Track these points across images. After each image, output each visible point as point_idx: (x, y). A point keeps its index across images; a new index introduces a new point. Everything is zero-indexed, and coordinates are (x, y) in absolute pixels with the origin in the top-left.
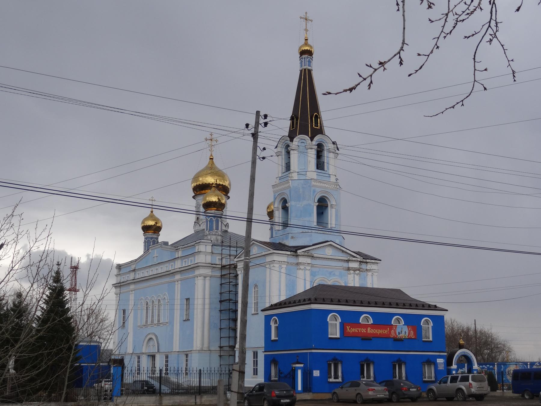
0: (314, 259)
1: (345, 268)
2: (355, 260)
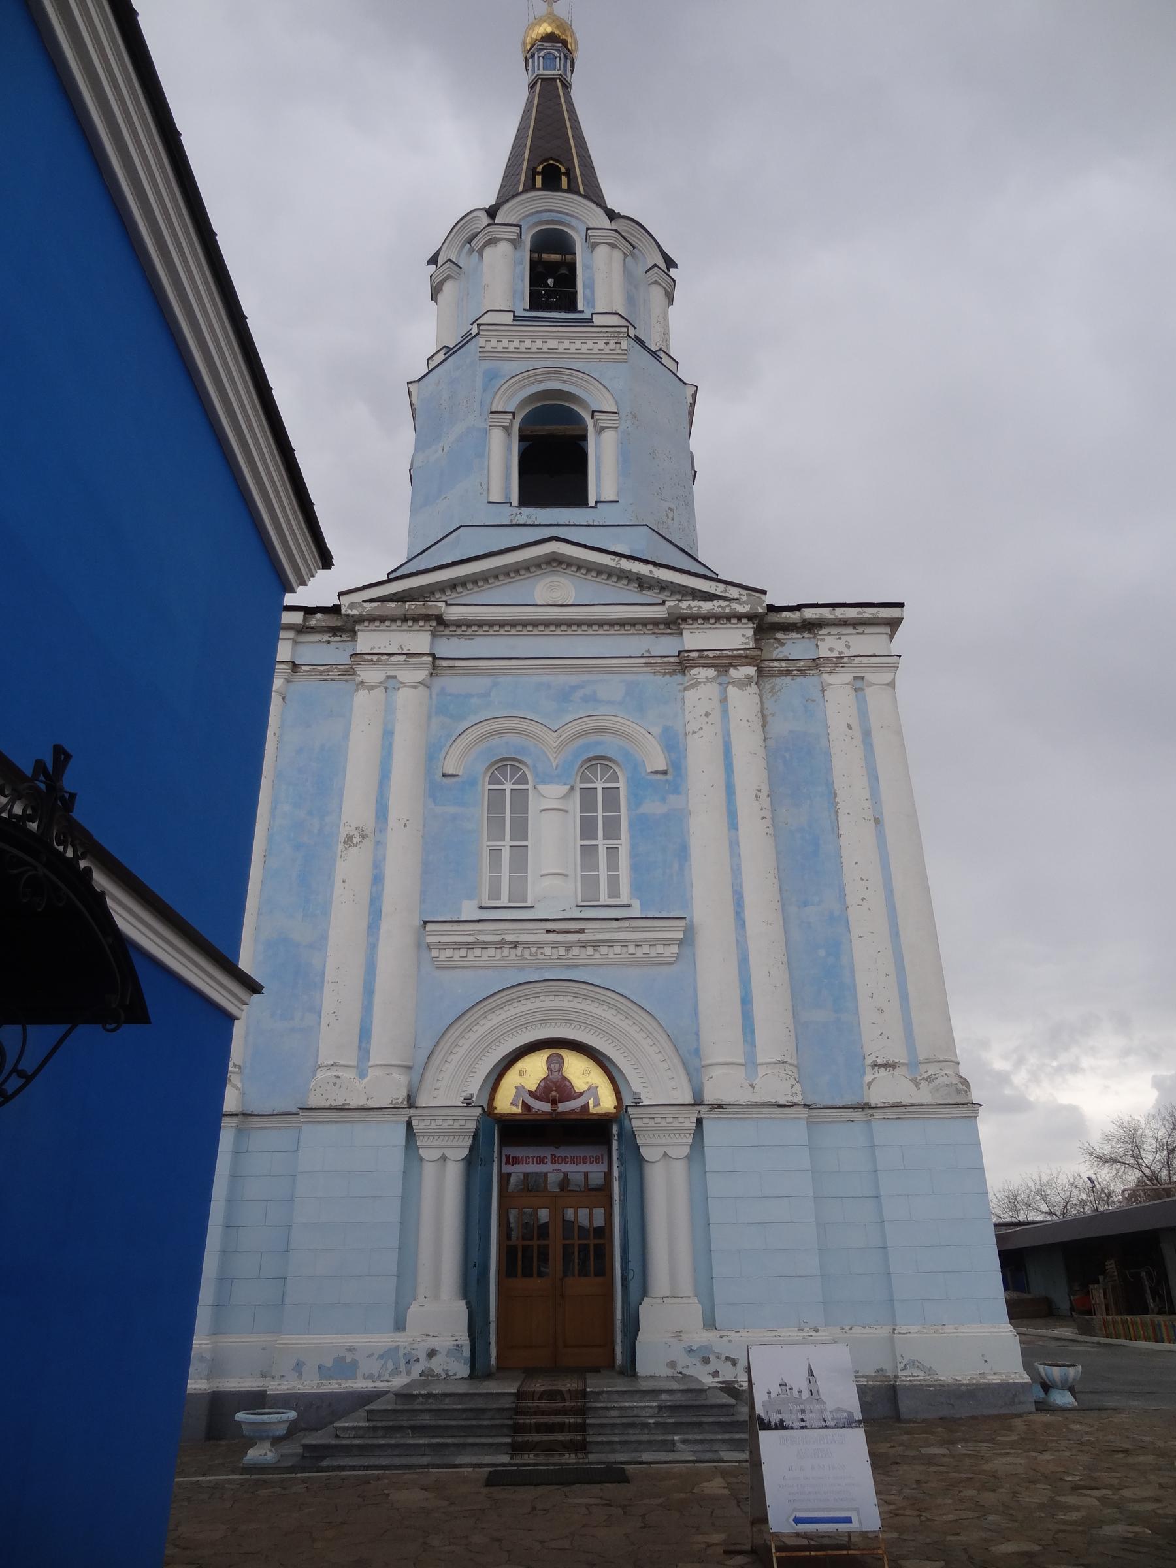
0: (460, 636)
1: (659, 660)
2: (717, 610)
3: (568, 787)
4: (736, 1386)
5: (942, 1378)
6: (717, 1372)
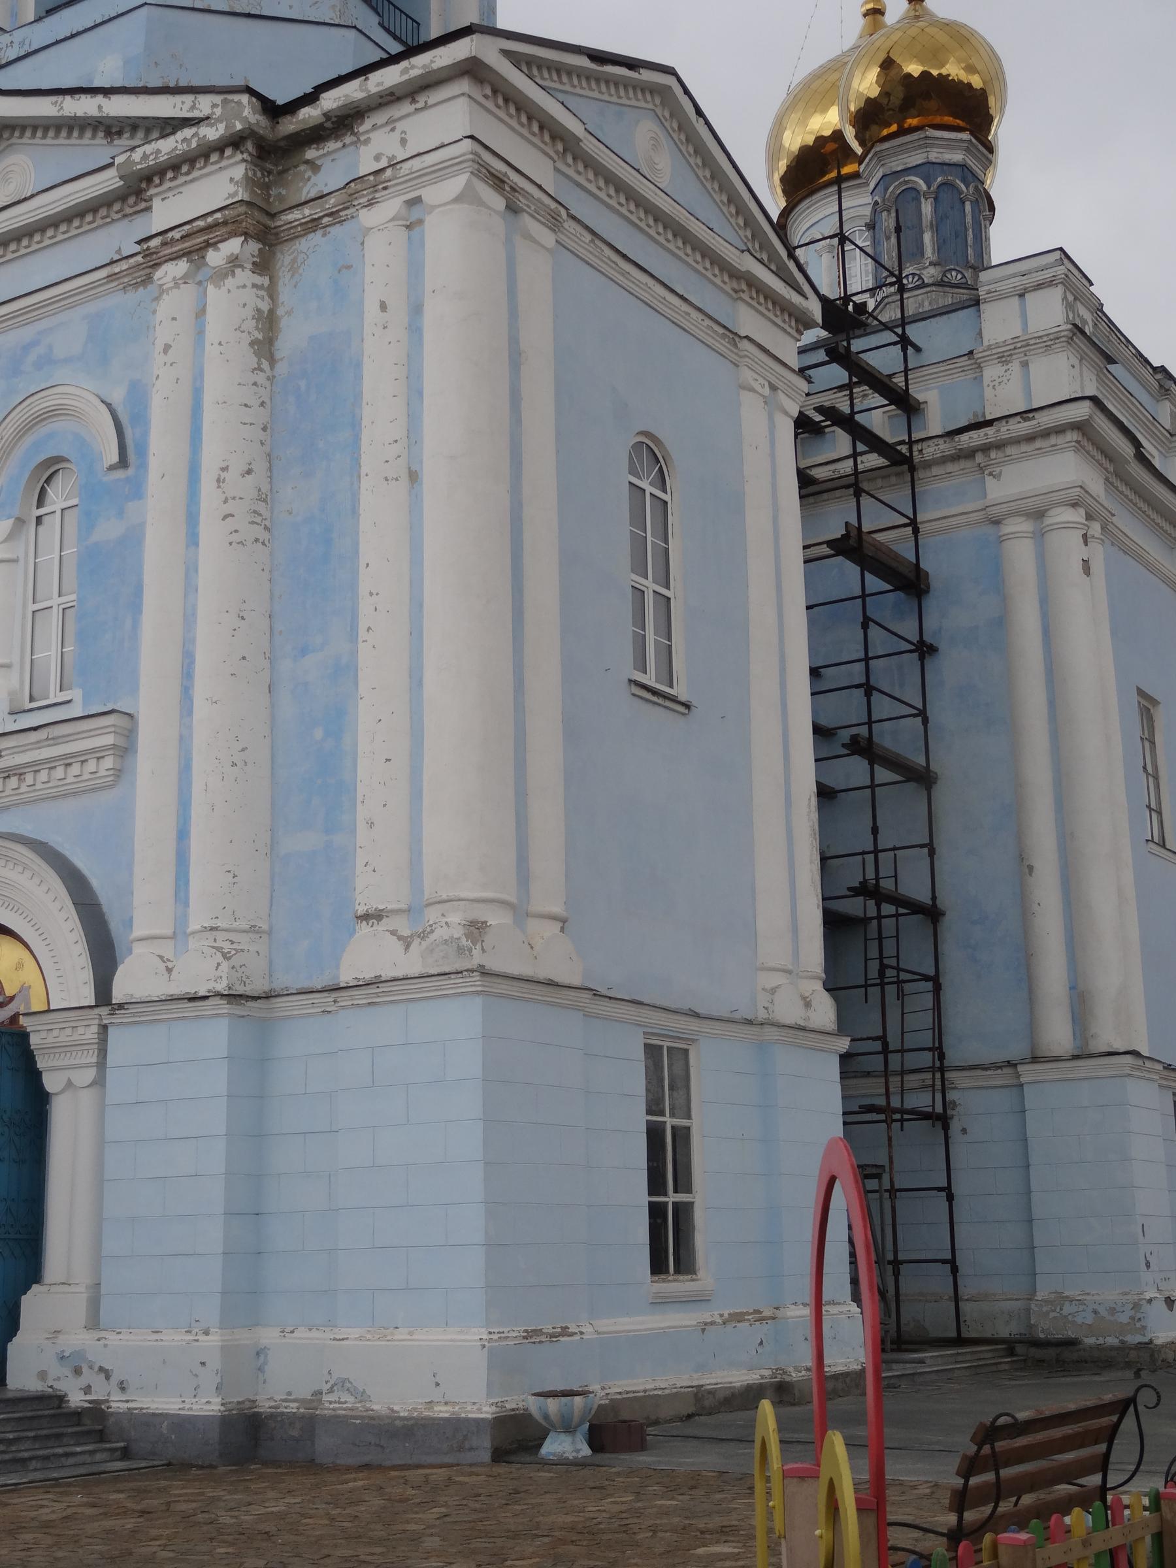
1: (124, 265)
3: (11, 521)
4: (103, 1407)
5: (375, 1407)
6: (89, 1387)
